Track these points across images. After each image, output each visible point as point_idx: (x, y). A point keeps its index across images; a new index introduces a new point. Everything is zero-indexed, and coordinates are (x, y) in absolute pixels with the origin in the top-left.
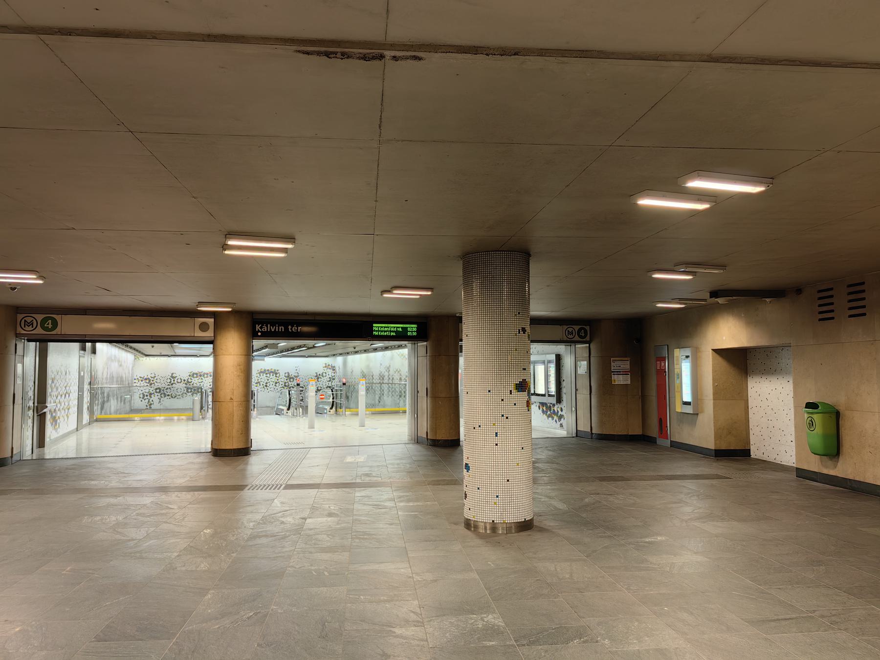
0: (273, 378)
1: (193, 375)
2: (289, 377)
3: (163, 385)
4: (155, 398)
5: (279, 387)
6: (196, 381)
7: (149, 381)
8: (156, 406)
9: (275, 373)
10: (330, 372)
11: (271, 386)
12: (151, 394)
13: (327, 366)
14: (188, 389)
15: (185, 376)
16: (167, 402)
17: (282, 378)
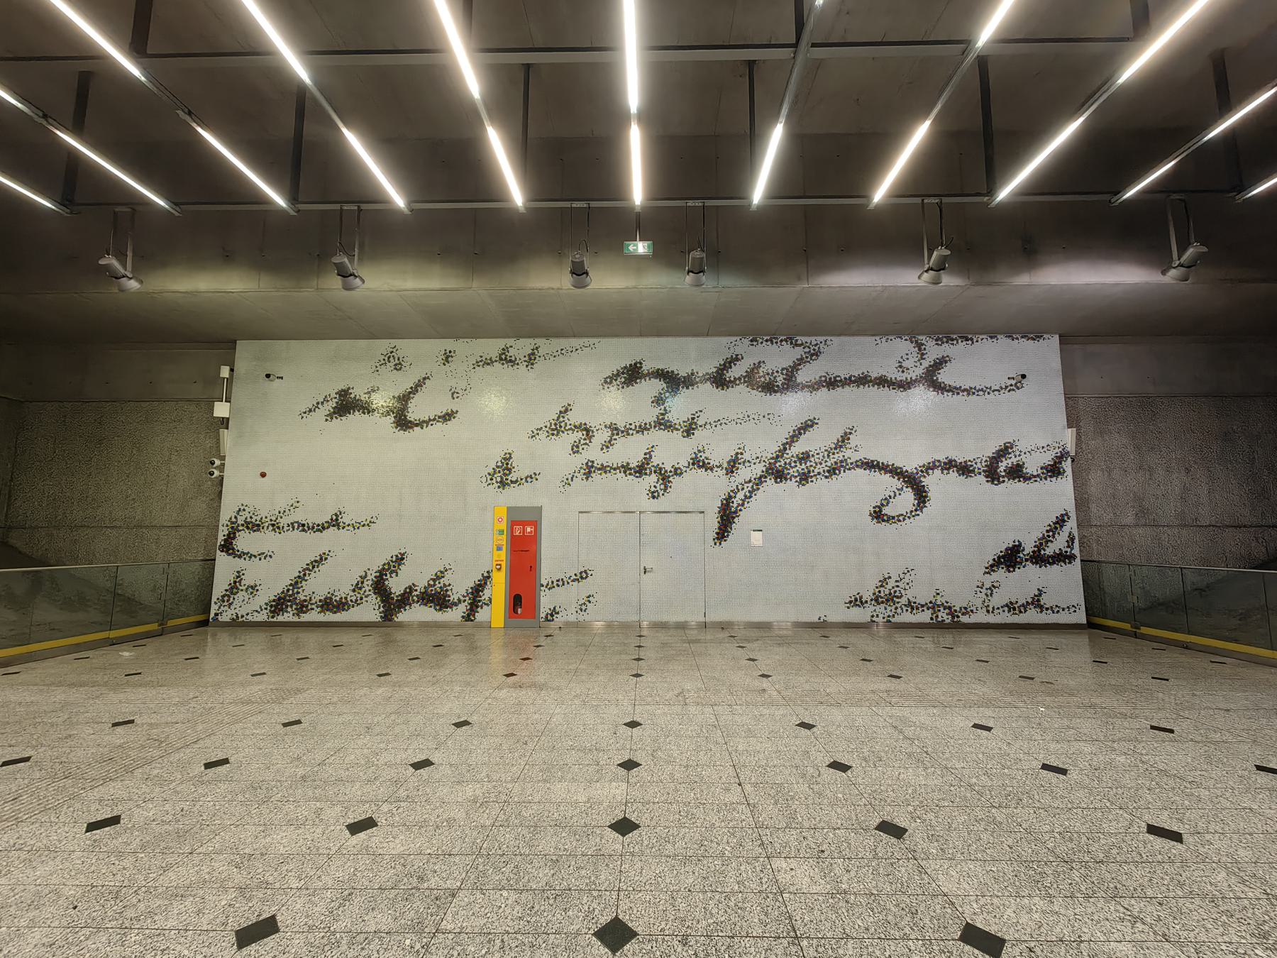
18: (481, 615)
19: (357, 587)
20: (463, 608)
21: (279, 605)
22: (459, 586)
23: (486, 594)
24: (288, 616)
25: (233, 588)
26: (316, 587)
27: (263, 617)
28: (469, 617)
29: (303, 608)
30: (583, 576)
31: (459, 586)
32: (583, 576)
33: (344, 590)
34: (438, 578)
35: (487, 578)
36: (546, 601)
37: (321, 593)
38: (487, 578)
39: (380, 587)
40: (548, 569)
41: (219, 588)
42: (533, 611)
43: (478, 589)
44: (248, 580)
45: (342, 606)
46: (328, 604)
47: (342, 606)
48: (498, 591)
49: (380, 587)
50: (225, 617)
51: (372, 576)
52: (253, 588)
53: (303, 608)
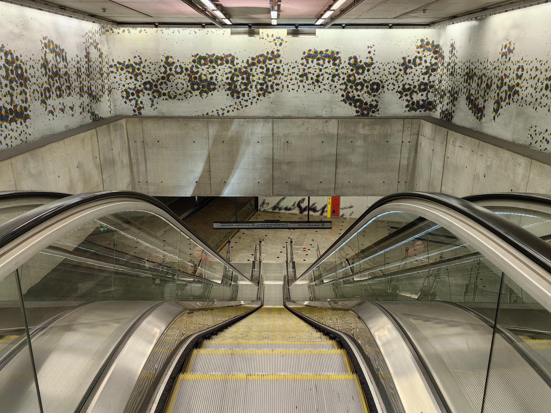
0: (329, 67)
1: (200, 60)
2: (357, 66)
3: (155, 77)
4: (145, 98)
5: (338, 84)
6: (204, 71)
7: (133, 68)
8: (147, 111)
9: (333, 57)
10: (429, 56)
11: (326, 81)
12: (138, 92)
13: (424, 45)
14: (192, 85)
15: (187, 62)
16: (165, 107)
17: (345, 69)
18: (325, 214)
19: (293, 205)
20: (320, 212)
21: (274, 208)
22: (319, 207)
23: (326, 209)
24: (277, 211)
25: (263, 203)
26: (283, 204)
27: (271, 210)
28: (321, 214)
29: (280, 209)
30: (351, 207)
31: (319, 207)
32: (351, 207)
33: (290, 205)
34: (313, 205)
35: (326, 206)
36: (341, 212)
37: (284, 206)
38: (326, 206)
39: (299, 205)
40: (342, 205)
41: (260, 203)
42: (338, 214)
43: (324, 208)
44: (266, 202)
45: (290, 209)
46: (286, 209)
47: (290, 209)
48: (329, 208)
49: (299, 205)
50: (262, 210)
51: (297, 203)
52: (268, 204)
53: (280, 209)
